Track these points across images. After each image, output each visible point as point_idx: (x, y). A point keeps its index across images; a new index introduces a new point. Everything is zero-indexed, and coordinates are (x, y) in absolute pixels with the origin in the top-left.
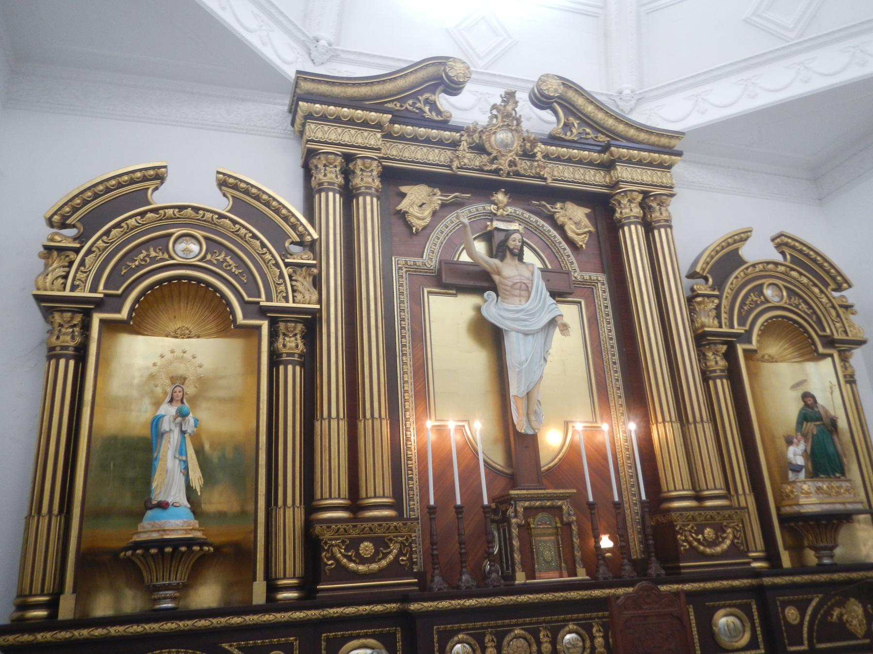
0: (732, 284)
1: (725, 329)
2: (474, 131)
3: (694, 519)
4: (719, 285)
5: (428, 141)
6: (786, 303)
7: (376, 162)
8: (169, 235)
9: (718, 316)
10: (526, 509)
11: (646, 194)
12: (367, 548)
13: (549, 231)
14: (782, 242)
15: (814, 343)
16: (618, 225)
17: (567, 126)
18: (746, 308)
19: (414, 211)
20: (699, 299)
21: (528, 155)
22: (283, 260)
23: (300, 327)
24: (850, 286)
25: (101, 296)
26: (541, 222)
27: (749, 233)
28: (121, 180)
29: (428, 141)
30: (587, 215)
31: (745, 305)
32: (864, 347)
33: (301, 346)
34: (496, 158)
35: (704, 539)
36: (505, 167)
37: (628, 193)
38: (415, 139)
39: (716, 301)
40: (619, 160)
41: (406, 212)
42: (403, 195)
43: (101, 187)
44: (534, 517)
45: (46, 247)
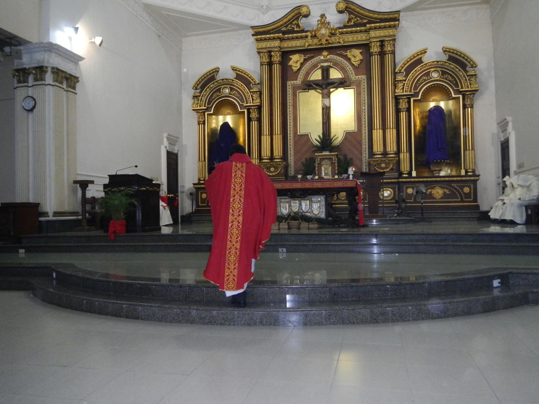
0: (413, 74)
1: (404, 93)
2: (313, 31)
3: (377, 161)
4: (407, 76)
5: (297, 38)
6: (440, 78)
7: (277, 52)
8: (221, 88)
9: (403, 88)
10: (320, 159)
11: (382, 41)
12: (272, 169)
13: (344, 62)
14: (446, 51)
15: (451, 93)
16: (371, 54)
17: (350, 20)
18: (419, 82)
19: (294, 65)
20: (396, 82)
21: (332, 34)
22: (249, 91)
23: (256, 110)
24: (476, 67)
25: (206, 108)
26: (341, 59)
27: (426, 50)
28: (207, 74)
29: (297, 38)
30: (360, 53)
31: (420, 81)
32: (478, 91)
33: (257, 116)
34: (321, 40)
35: (381, 167)
36: (324, 42)
37: (373, 43)
38: (293, 38)
39: (404, 82)
40: (371, 29)
41: (291, 66)
42: (291, 59)
43: (203, 77)
44: (323, 161)
45: (193, 96)
